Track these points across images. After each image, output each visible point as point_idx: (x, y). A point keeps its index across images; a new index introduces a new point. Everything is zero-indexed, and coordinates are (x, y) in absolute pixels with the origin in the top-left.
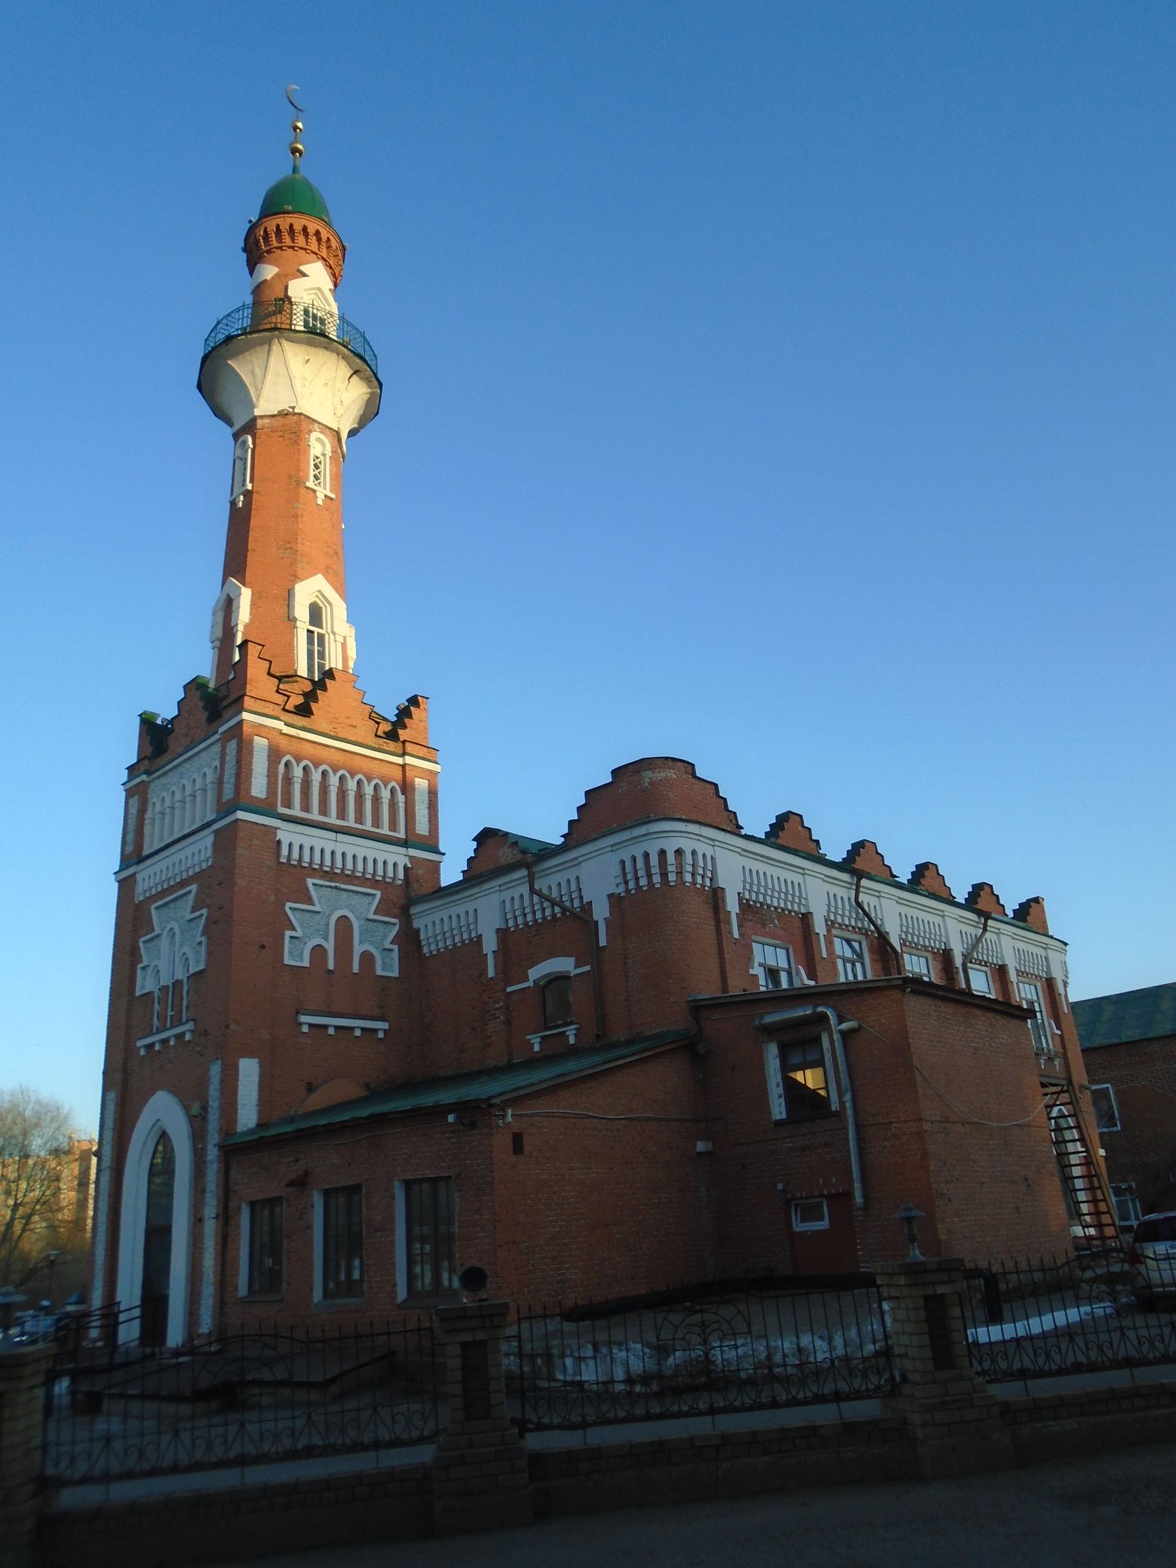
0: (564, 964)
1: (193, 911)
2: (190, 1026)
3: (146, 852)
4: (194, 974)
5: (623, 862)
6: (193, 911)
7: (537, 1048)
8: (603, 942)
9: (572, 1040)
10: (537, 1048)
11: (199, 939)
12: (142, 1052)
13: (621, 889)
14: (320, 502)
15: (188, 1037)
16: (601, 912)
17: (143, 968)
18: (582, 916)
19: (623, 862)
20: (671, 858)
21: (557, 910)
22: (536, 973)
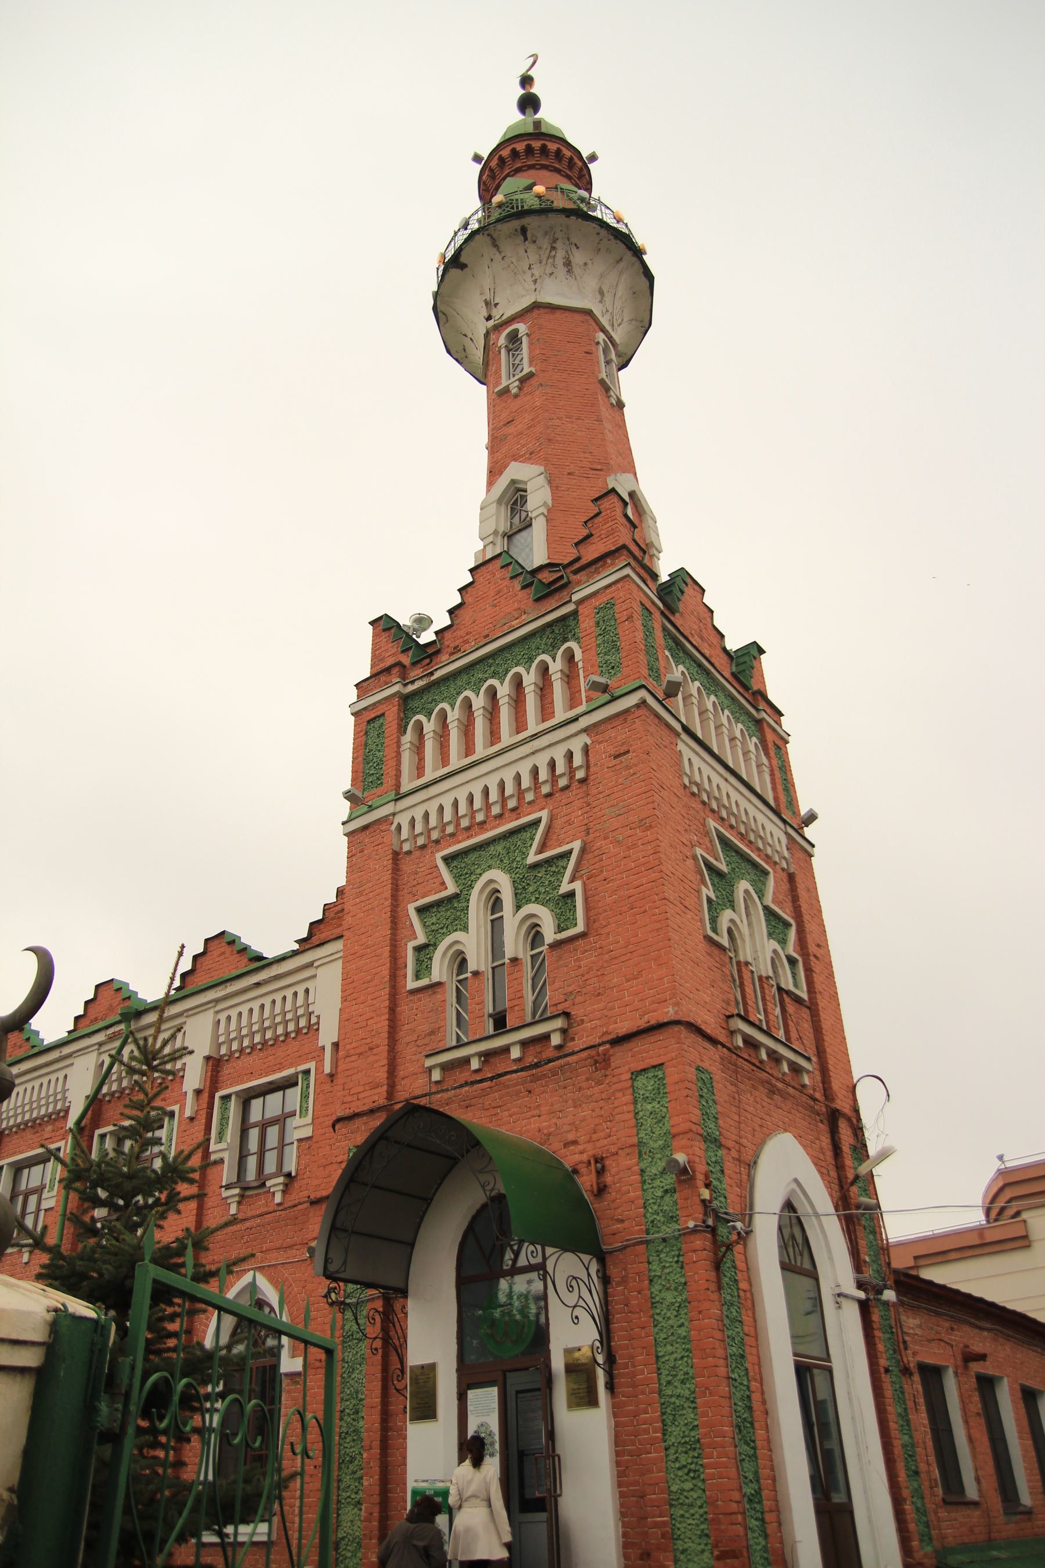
1: (540, 851)
2: (559, 1023)
3: (405, 788)
4: (556, 945)
11: (565, 888)
12: (436, 1075)
15: (556, 1040)
17: (418, 949)
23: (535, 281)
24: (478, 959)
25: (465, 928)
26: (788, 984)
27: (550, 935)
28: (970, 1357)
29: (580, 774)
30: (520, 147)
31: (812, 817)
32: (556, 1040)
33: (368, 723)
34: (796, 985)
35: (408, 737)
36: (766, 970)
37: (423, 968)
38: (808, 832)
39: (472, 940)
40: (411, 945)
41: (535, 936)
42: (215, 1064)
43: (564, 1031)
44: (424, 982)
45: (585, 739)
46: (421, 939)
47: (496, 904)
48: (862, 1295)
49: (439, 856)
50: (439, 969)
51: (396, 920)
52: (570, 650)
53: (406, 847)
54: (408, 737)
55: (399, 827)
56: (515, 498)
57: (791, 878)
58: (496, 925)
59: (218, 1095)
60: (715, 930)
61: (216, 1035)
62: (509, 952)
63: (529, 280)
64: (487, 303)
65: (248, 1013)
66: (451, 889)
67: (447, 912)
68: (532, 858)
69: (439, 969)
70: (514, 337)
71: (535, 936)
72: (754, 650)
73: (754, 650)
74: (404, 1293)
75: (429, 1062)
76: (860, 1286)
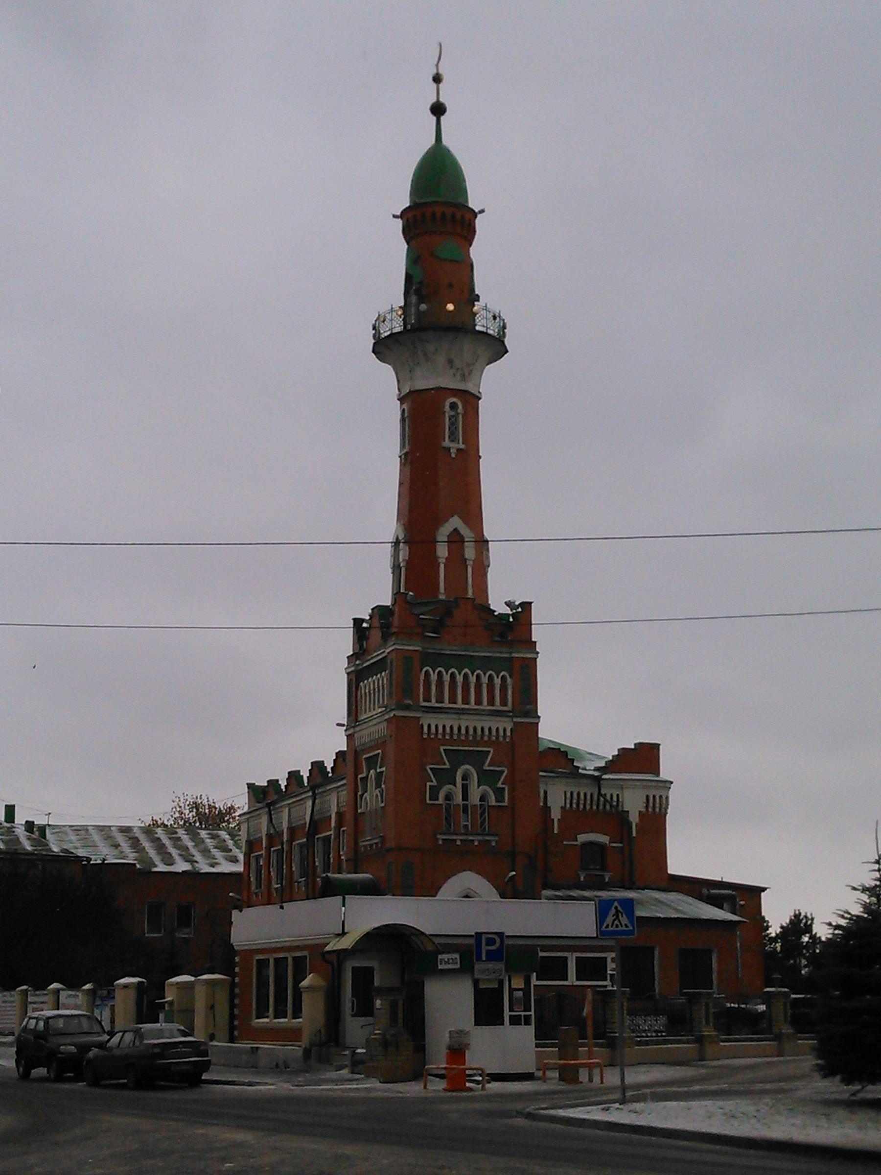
0: (604, 839)
5: (647, 797)
7: (582, 879)
8: (634, 834)
9: (607, 880)
10: (582, 879)
11: (500, 785)
12: (440, 842)
13: (644, 810)
14: (453, 456)
16: (634, 818)
18: (622, 817)
19: (647, 797)
20: (657, 798)
21: (608, 807)
22: (582, 838)
32: (494, 844)
37: (434, 796)
40: (428, 784)
43: (497, 841)
46: (435, 783)
50: (441, 800)
53: (425, 736)
58: (465, 789)
66: (448, 766)
68: (486, 767)
69: (441, 800)
70: (453, 406)
71: (483, 798)
75: (439, 836)
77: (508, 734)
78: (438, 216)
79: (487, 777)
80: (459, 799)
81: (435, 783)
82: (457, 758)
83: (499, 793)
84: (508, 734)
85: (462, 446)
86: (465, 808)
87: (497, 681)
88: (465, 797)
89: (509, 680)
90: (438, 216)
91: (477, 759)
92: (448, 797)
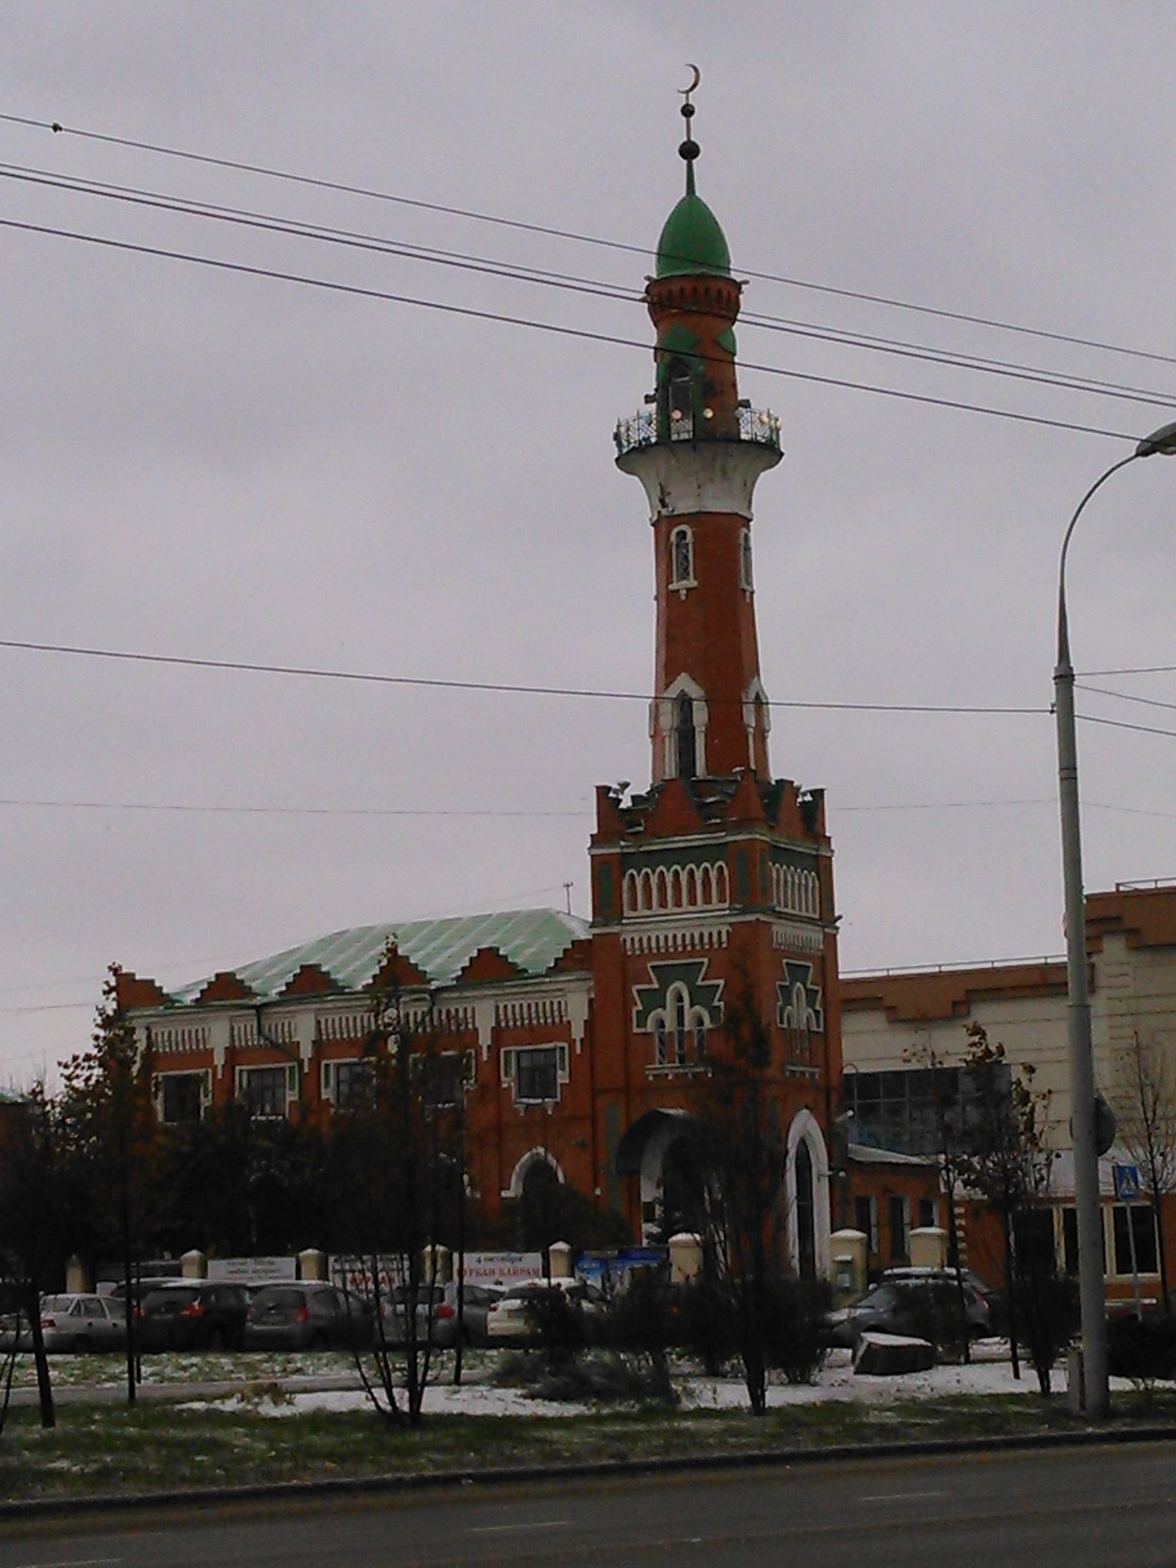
1: (703, 980)
6: (703, 980)
11: (716, 1003)
12: (651, 1078)
17: (638, 1012)
23: (699, 486)
24: (670, 1026)
25: (664, 1007)
26: (814, 1028)
27: (708, 1024)
28: (886, 1191)
29: (724, 946)
30: (688, 287)
31: (840, 917)
33: (600, 867)
34: (818, 1027)
35: (626, 883)
36: (804, 1027)
37: (642, 1022)
38: (838, 924)
39: (668, 1015)
41: (700, 1022)
42: (497, 1032)
44: (642, 1030)
45: (728, 927)
46: (640, 1008)
47: (680, 999)
48: (830, 1173)
49: (649, 965)
50: (650, 1027)
51: (626, 992)
52: (721, 867)
53: (629, 953)
54: (626, 883)
55: (625, 941)
56: (684, 703)
57: (823, 959)
58: (680, 1011)
59: (502, 1050)
60: (782, 1022)
61: (497, 1016)
62: (686, 1029)
63: (695, 485)
64: (662, 489)
65: (517, 1003)
66: (656, 986)
67: (655, 999)
68: (699, 983)
69: (650, 1027)
70: (682, 535)
72: (818, 794)
73: (818, 794)
74: (638, 1172)
76: (830, 1169)
77: (724, 938)
78: (693, 294)
79: (700, 996)
80: (670, 1026)
81: (640, 1008)
82: (666, 975)
83: (714, 1012)
84: (724, 938)
85: (692, 583)
86: (681, 1033)
87: (713, 875)
88: (681, 1022)
89: (726, 872)
90: (693, 294)
91: (688, 973)
92: (662, 1024)
